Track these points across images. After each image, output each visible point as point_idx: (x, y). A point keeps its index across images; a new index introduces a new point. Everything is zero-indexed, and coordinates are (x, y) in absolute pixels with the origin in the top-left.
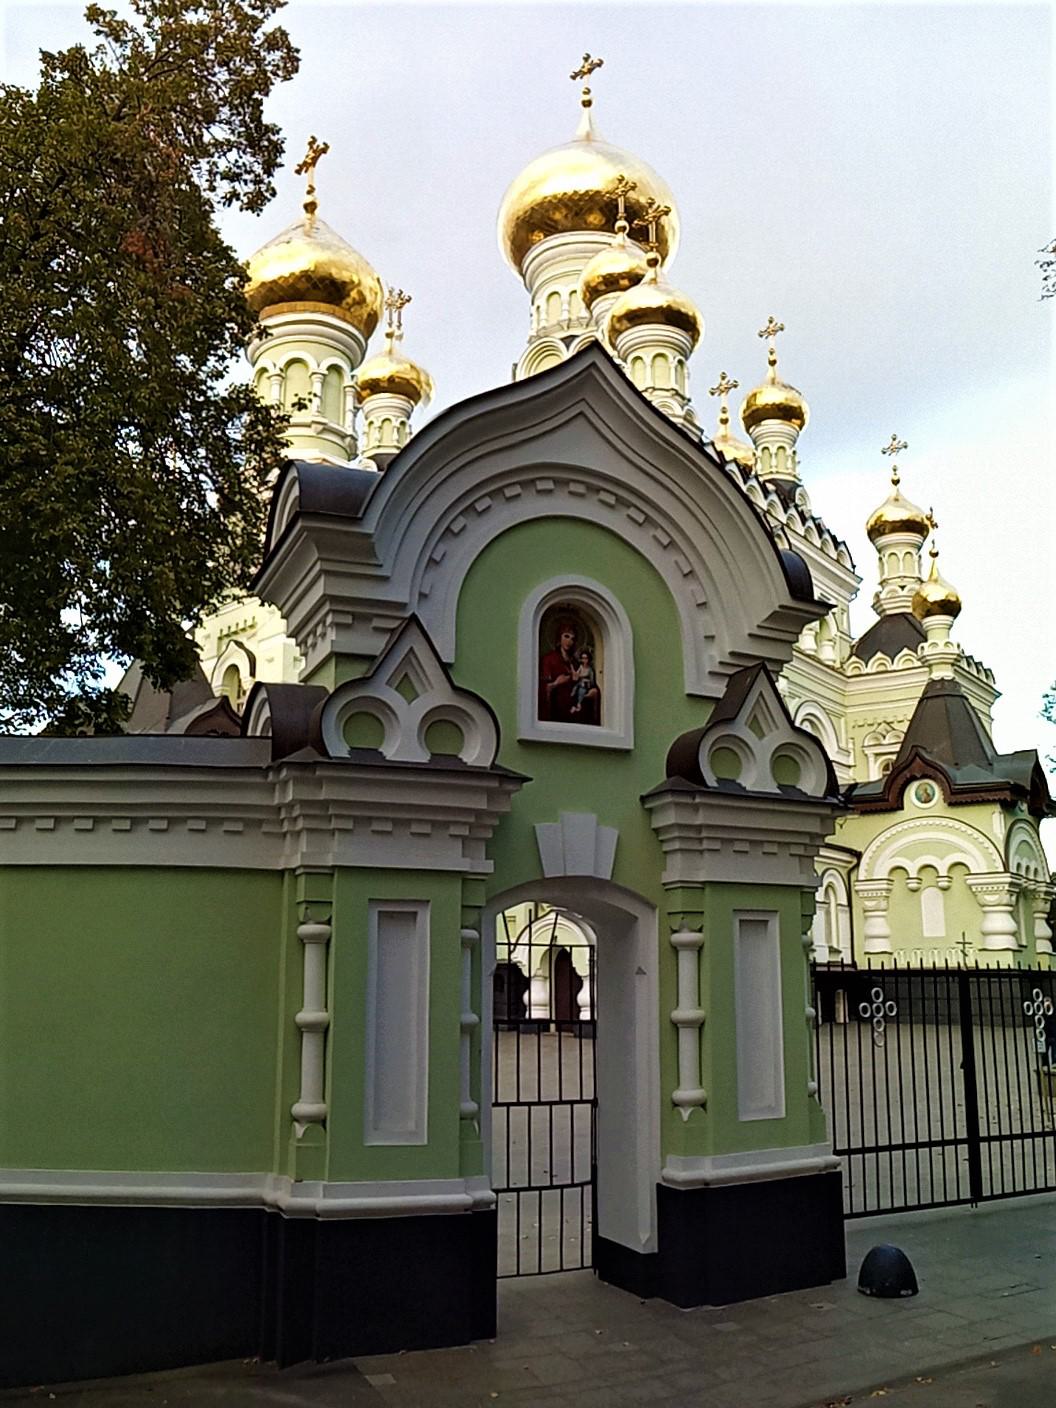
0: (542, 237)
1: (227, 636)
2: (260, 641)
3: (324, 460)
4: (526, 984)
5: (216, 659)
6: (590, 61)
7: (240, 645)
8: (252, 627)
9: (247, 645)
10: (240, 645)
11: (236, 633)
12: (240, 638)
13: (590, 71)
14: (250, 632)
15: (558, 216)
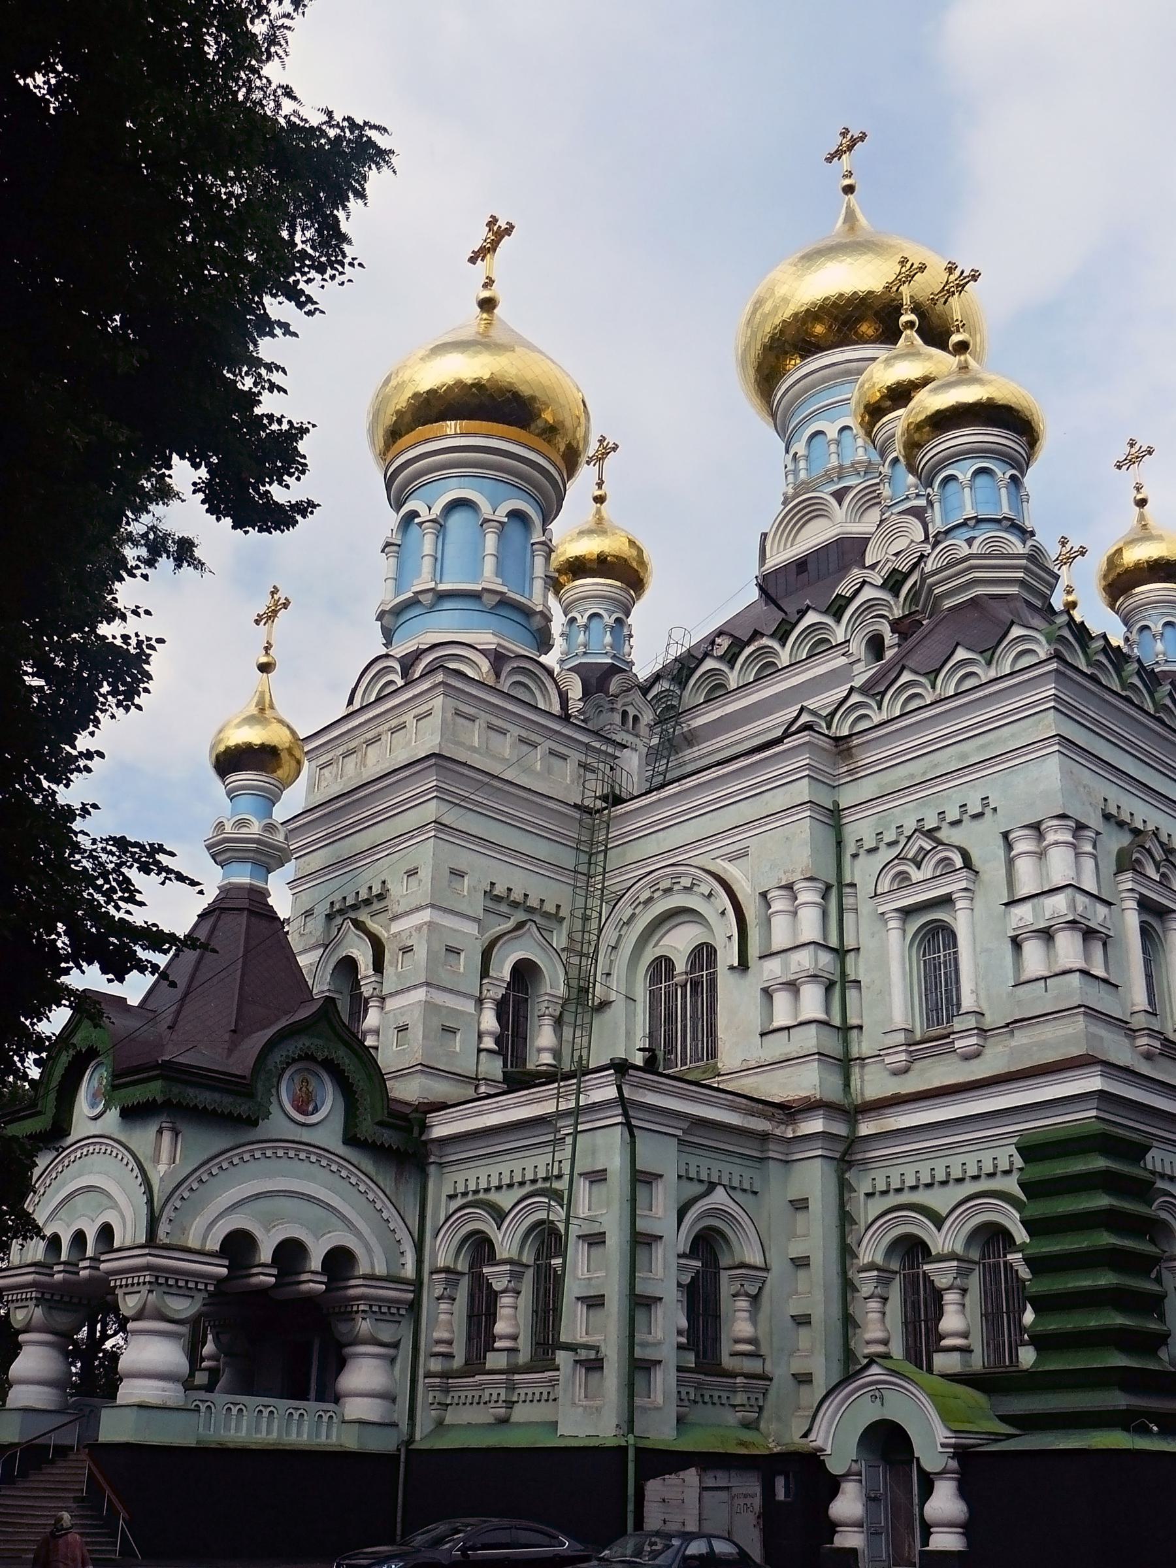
0: (798, 361)
1: (341, 912)
2: (395, 918)
3: (499, 645)
4: (833, 1486)
5: (322, 950)
6: (849, 137)
7: (359, 925)
8: (381, 897)
9: (373, 926)
10: (358, 925)
11: (354, 907)
12: (363, 916)
13: (850, 148)
14: (377, 906)
15: (819, 329)
